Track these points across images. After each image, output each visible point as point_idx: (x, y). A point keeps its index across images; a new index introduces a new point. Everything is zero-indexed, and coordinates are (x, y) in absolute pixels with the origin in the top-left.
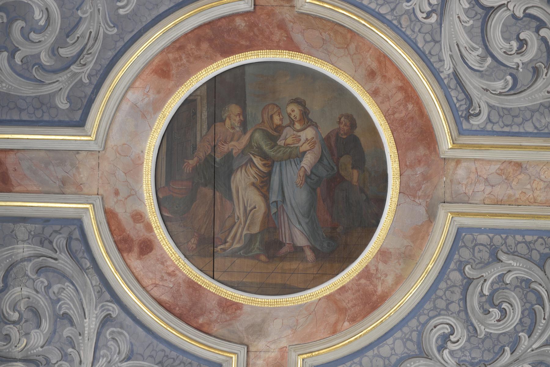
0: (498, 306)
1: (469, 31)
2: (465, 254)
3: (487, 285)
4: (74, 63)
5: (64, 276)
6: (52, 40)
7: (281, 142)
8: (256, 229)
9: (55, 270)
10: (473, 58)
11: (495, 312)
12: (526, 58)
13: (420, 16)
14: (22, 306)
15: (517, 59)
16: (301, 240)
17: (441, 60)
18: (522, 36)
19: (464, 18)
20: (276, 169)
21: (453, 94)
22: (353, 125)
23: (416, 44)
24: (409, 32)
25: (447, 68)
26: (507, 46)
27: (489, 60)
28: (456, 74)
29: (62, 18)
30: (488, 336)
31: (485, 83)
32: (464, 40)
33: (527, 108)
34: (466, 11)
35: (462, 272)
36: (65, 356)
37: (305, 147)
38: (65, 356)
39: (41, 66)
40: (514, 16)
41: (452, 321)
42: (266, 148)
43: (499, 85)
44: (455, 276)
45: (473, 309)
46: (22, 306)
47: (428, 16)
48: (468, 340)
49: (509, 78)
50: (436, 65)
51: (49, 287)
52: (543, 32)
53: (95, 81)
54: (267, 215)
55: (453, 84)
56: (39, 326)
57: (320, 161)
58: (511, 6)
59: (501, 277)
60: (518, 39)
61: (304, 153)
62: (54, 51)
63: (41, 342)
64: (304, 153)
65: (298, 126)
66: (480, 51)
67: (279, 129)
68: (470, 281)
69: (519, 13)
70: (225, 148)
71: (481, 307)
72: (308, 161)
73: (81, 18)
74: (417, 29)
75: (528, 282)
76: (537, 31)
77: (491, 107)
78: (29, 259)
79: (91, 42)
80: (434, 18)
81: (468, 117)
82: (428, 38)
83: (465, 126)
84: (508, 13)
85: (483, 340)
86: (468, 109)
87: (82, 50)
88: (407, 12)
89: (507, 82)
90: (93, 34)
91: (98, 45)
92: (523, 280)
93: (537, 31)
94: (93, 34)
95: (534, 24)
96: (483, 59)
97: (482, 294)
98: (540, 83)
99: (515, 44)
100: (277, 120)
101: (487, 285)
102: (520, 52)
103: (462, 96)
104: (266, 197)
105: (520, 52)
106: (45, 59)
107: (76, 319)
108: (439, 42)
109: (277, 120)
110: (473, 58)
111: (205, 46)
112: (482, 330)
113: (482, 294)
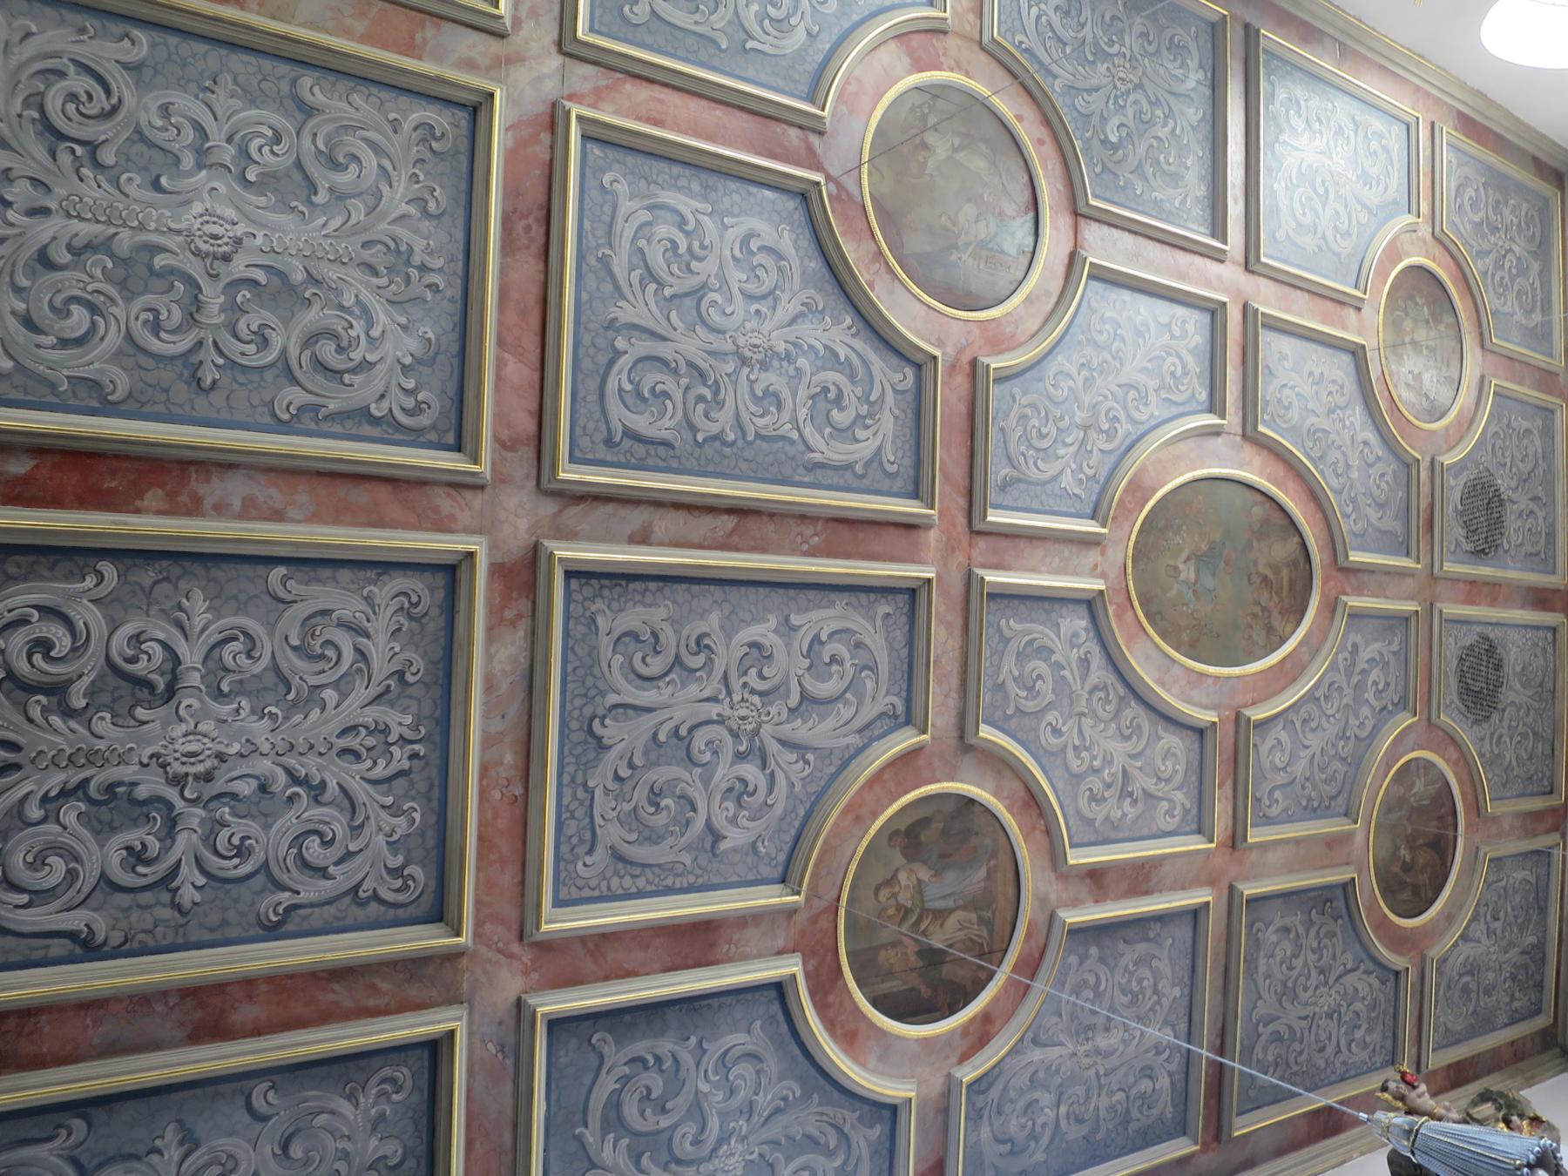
0: (1035, 682)
1: (822, 718)
2: (998, 714)
3: (1019, 692)
4: (842, 1130)
5: (1005, 1090)
6: (822, 1159)
7: (909, 904)
8: (974, 917)
9: (1000, 1099)
10: (847, 713)
11: (1039, 684)
12: (847, 655)
13: (807, 772)
14: (1023, 1121)
15: (848, 665)
16: (982, 873)
17: (847, 747)
18: (827, 660)
19: (810, 724)
20: (929, 905)
21: (876, 733)
22: (896, 833)
23: (832, 775)
24: (822, 783)
25: (854, 740)
26: (835, 676)
27: (848, 695)
28: (861, 731)
29: (803, 1154)
30: (1054, 691)
31: (868, 699)
32: (830, 723)
33: (889, 655)
34: (805, 721)
35: (1012, 716)
36: (1057, 1071)
37: (913, 879)
38: (1057, 1071)
39: (845, 1163)
40: (809, 669)
41: (1043, 724)
42: (914, 918)
43: (869, 685)
44: (1014, 722)
45: (1036, 706)
46: (1023, 1121)
47: (807, 762)
48: (1056, 709)
49: (863, 674)
50: (852, 751)
51: (1012, 1101)
52: (824, 637)
53: (858, 1105)
54: (963, 908)
55: (868, 733)
56: (1037, 1101)
57: (925, 862)
58: (800, 672)
59: (1015, 679)
60: (830, 664)
61: (918, 880)
62: (831, 1154)
63: (1047, 1095)
64: (918, 880)
65: (897, 889)
66: (840, 705)
67: (899, 907)
68: (1017, 709)
69: (807, 662)
70: (913, 958)
71: (1034, 698)
72: (924, 874)
73: (804, 1135)
74: (819, 774)
75: (1019, 654)
76: (822, 643)
77: (887, 693)
78: (991, 1125)
79: (825, 1118)
80: (810, 757)
81: (895, 717)
82: (827, 762)
83: (902, 719)
84: (806, 675)
85: (1056, 695)
86: (890, 717)
87: (832, 1125)
88: (804, 786)
89: (867, 676)
90: (818, 1118)
91: (828, 1110)
92: (1017, 659)
93: (822, 643)
94: (818, 1118)
95: (816, 646)
96: (847, 703)
97: (1026, 698)
98: (868, 641)
99: (835, 668)
100: (891, 911)
101: (1019, 692)
102: (841, 663)
103: (878, 724)
104: (951, 911)
105: (841, 663)
106: (838, 1162)
107: (1033, 1069)
108: (831, 750)
109: (891, 911)
110: (847, 713)
111: (831, 998)
112: (1050, 697)
113: (1026, 698)
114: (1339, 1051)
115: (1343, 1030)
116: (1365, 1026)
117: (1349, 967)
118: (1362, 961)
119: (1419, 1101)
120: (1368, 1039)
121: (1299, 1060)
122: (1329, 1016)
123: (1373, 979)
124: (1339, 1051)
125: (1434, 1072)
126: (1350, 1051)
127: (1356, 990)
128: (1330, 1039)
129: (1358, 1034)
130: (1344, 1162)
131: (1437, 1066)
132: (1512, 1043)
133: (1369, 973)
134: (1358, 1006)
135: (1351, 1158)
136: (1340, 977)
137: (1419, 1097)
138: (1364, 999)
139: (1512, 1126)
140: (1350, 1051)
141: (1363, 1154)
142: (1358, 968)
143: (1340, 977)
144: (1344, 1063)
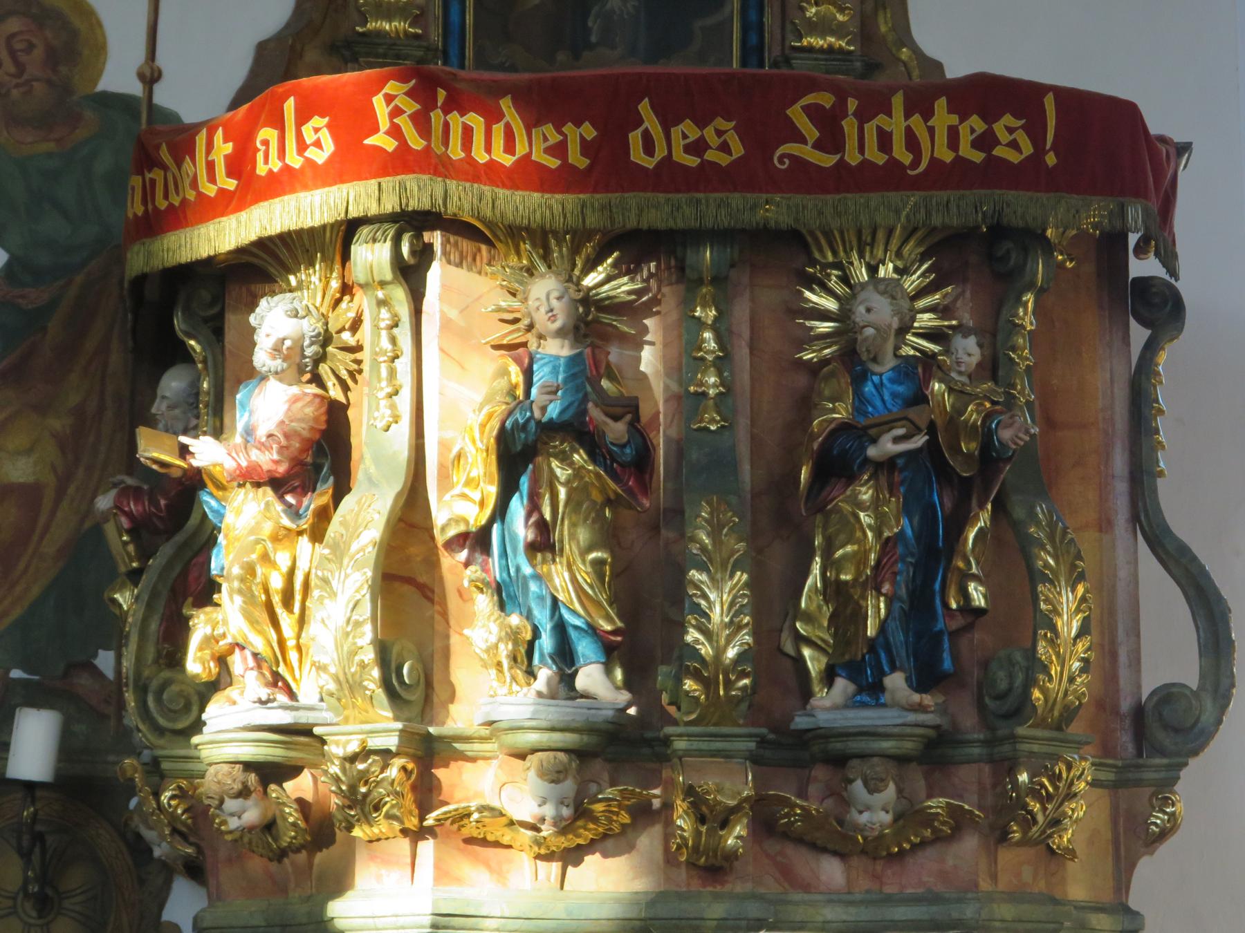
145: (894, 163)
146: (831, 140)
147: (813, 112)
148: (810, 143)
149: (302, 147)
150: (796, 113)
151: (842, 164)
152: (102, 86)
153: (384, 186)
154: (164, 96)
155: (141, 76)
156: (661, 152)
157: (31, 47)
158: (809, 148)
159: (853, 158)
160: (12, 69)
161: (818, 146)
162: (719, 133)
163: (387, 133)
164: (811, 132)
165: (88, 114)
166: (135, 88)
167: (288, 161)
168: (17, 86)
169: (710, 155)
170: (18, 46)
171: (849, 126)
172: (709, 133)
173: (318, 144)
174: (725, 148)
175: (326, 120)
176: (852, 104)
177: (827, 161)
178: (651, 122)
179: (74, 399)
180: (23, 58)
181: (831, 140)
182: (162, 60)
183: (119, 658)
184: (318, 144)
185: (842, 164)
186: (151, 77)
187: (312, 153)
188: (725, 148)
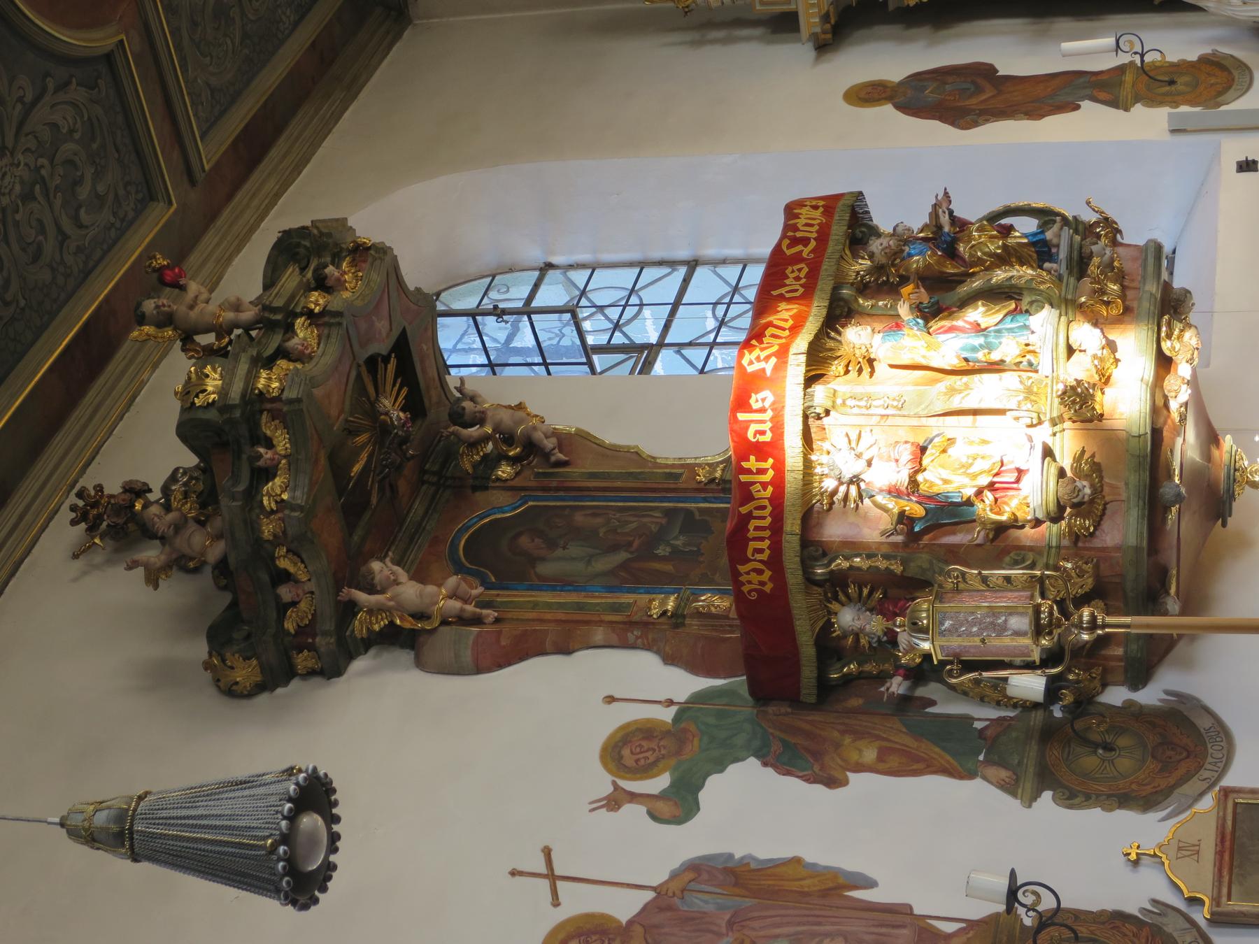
114: (63, 237)
115: (58, 202)
116: (89, 172)
117: (29, 98)
118: (47, 75)
119: (193, 314)
120: (101, 189)
121: (8, 297)
122: (28, 197)
123: (77, 93)
124: (63, 237)
125: (217, 166)
126: (81, 226)
127: (54, 126)
128: (42, 230)
129: (84, 192)
130: (134, 397)
131: (215, 159)
132: (313, 44)
133: (63, 86)
134: (69, 147)
135: (143, 384)
136: (21, 124)
137: (191, 307)
138: (71, 131)
139: (329, 283)
140: (81, 227)
141: (155, 366)
142: (44, 90)
143: (21, 124)
144: (79, 250)
145: (819, 224)
146: (805, 241)
147: (789, 247)
148: (803, 248)
149: (762, 410)
150: (789, 252)
151: (815, 239)
152: (670, 721)
153: (795, 351)
154: (682, 697)
155: (668, 706)
156: (798, 287)
157: (640, 746)
158: (806, 249)
159: (815, 235)
160: (651, 752)
161: (806, 246)
162: (793, 271)
163: (767, 362)
164: (799, 248)
165: (683, 725)
166: (674, 709)
167: (768, 419)
168: (660, 751)
169: (802, 274)
170: (638, 750)
171: (799, 234)
172: (792, 276)
173: (763, 400)
174: (800, 270)
175: (753, 395)
176: (790, 234)
177: (813, 244)
178: (783, 291)
179: (836, 734)
180: (646, 748)
181: (805, 241)
182: (662, 698)
183: (979, 719)
184: (763, 400)
185: (815, 239)
186: (670, 703)
187: (767, 404)
188: (800, 270)
